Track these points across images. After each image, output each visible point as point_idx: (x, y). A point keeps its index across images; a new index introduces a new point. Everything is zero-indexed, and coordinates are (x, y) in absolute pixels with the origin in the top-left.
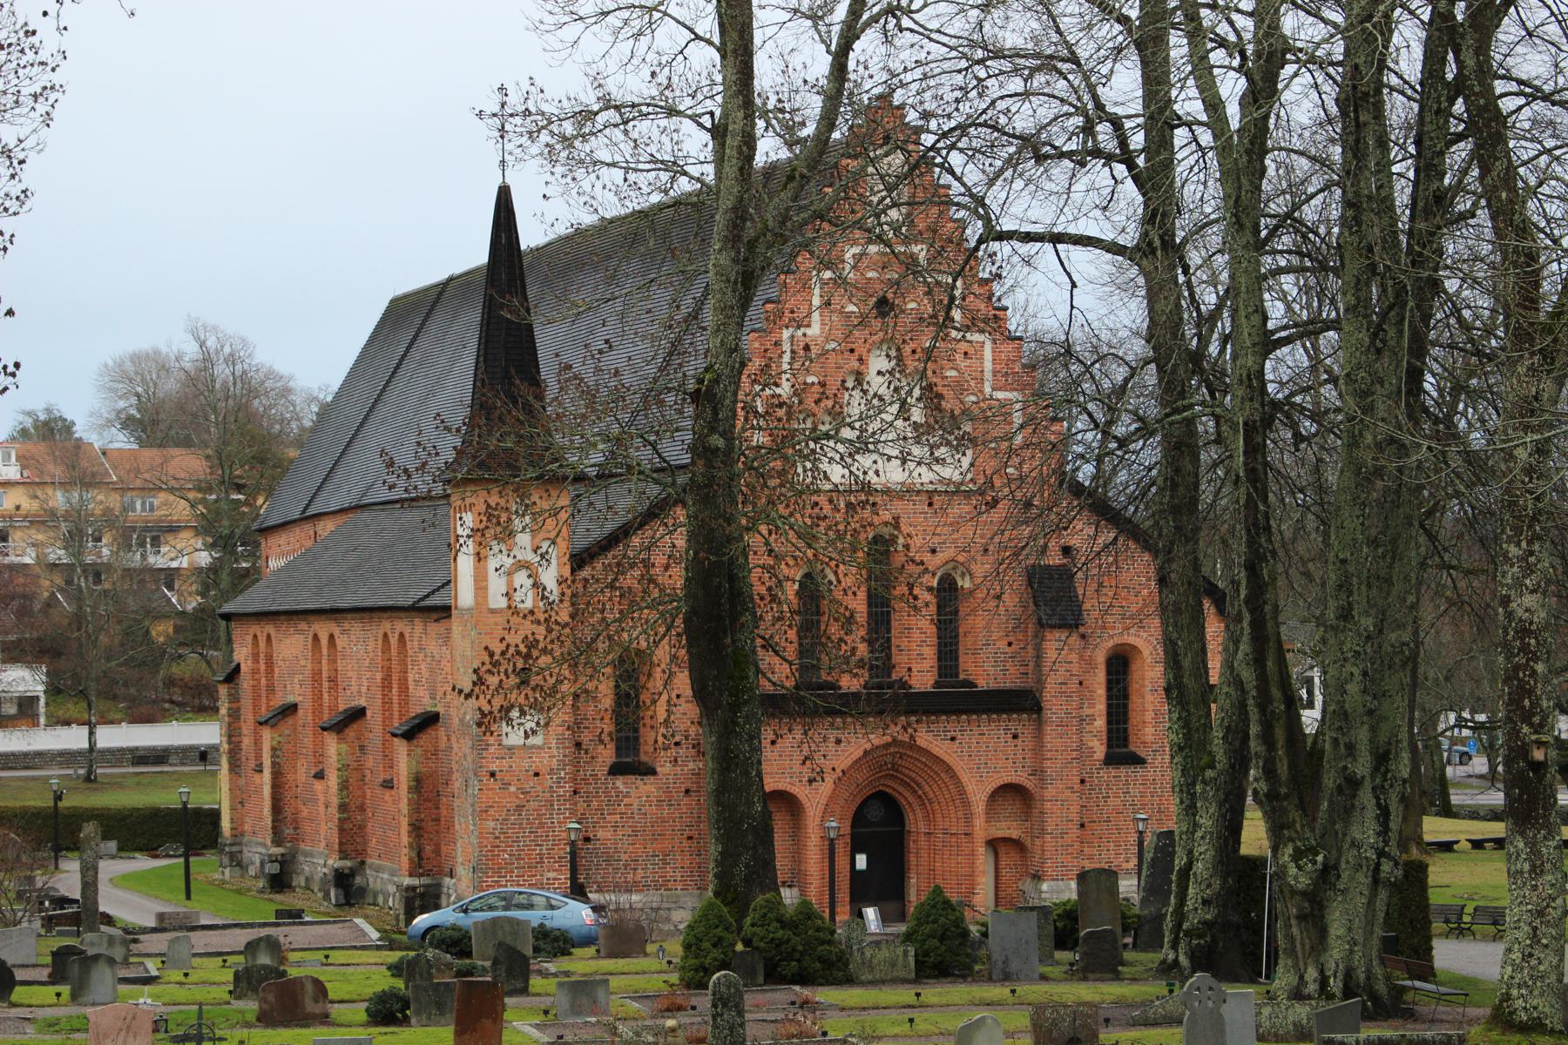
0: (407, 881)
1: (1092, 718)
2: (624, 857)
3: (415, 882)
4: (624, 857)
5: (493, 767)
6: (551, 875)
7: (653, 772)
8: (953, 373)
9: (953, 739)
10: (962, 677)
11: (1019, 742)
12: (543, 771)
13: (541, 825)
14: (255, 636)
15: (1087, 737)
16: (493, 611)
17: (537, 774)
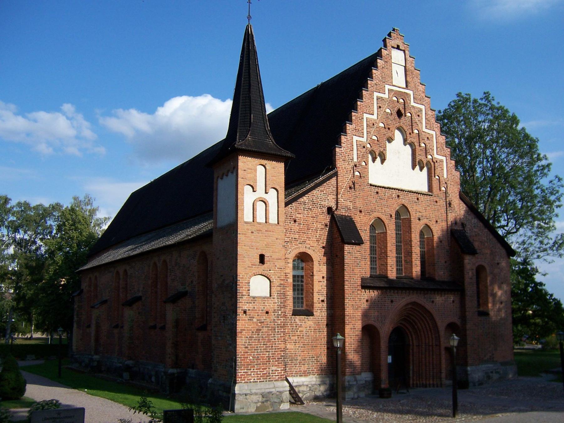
0: (171, 371)
2: (299, 358)
3: (175, 371)
4: (299, 358)
5: (245, 308)
6: (274, 368)
7: (313, 315)
12: (271, 311)
13: (269, 341)
14: (90, 278)
16: (246, 223)
17: (267, 313)
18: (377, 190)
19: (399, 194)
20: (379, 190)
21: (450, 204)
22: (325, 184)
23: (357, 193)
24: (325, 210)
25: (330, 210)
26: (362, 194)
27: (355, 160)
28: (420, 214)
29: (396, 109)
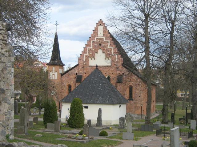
1: (126, 94)
8: (108, 52)
21: (118, 68)
25: (77, 74)
27: (84, 60)
29: (99, 44)
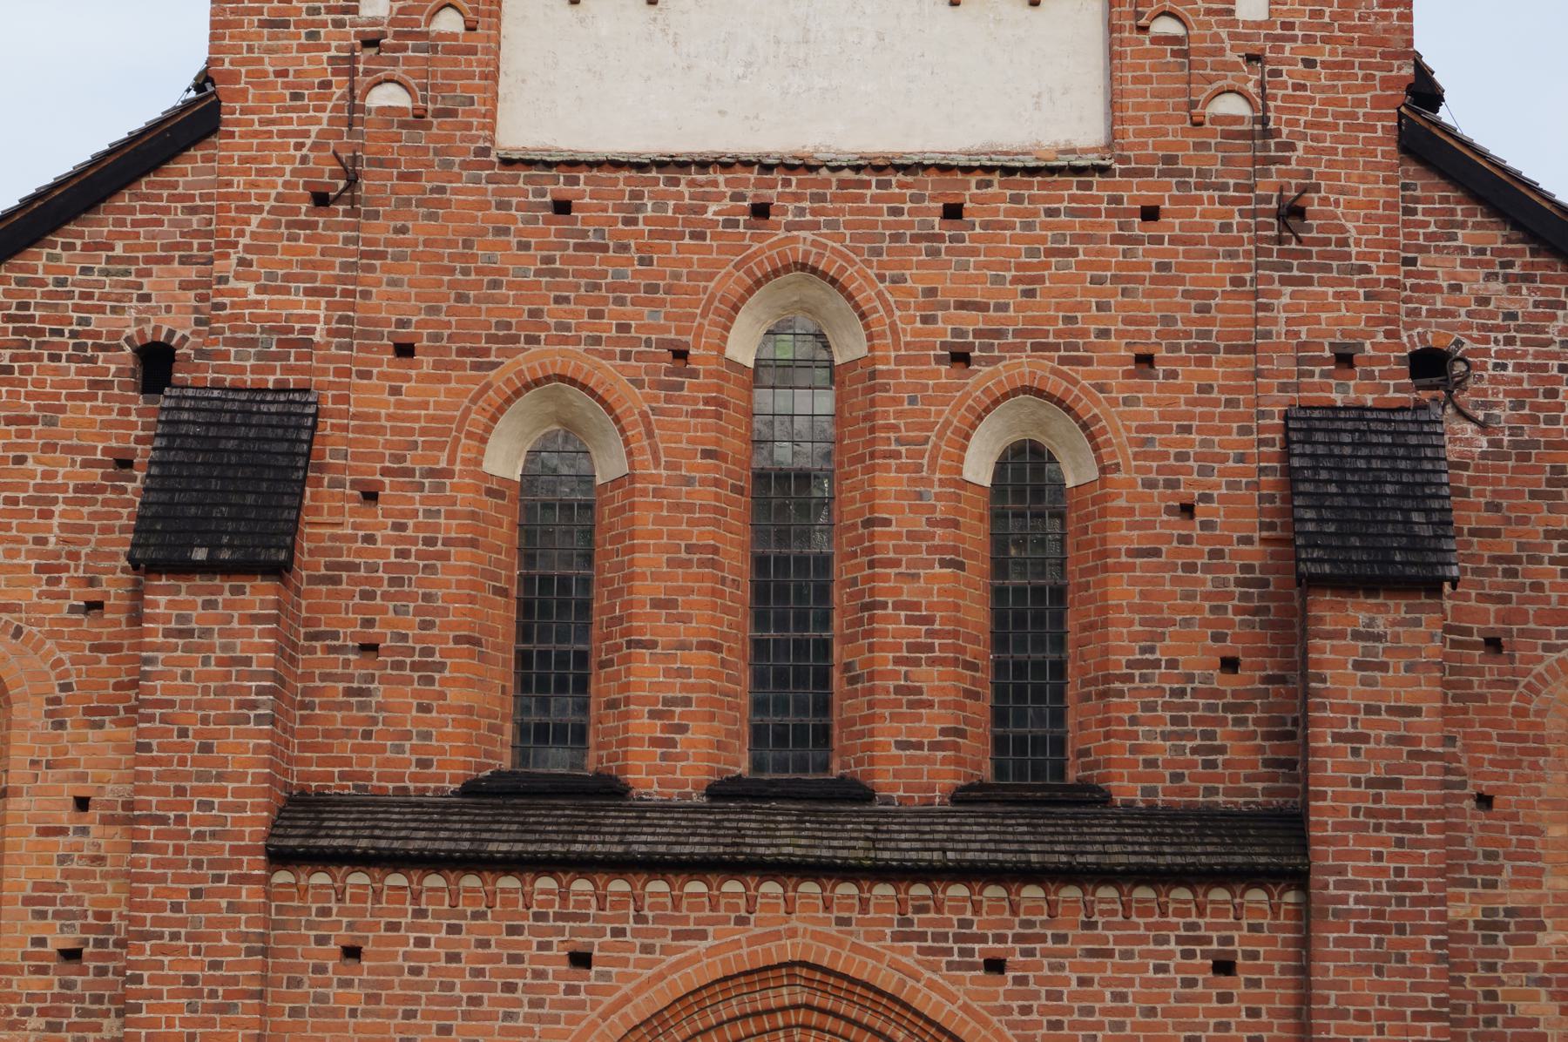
9: (995, 966)
10: (1072, 775)
11: (1237, 985)
15: (1510, 985)
18: (558, 187)
19: (770, 195)
20: (582, 189)
21: (1292, 213)
22: (125, 199)
23: (380, 231)
24: (118, 364)
25: (155, 363)
26: (419, 228)
28: (973, 321)
